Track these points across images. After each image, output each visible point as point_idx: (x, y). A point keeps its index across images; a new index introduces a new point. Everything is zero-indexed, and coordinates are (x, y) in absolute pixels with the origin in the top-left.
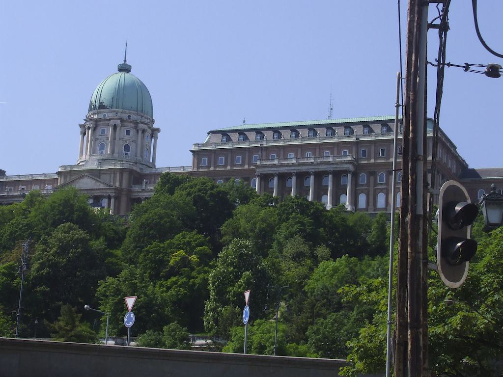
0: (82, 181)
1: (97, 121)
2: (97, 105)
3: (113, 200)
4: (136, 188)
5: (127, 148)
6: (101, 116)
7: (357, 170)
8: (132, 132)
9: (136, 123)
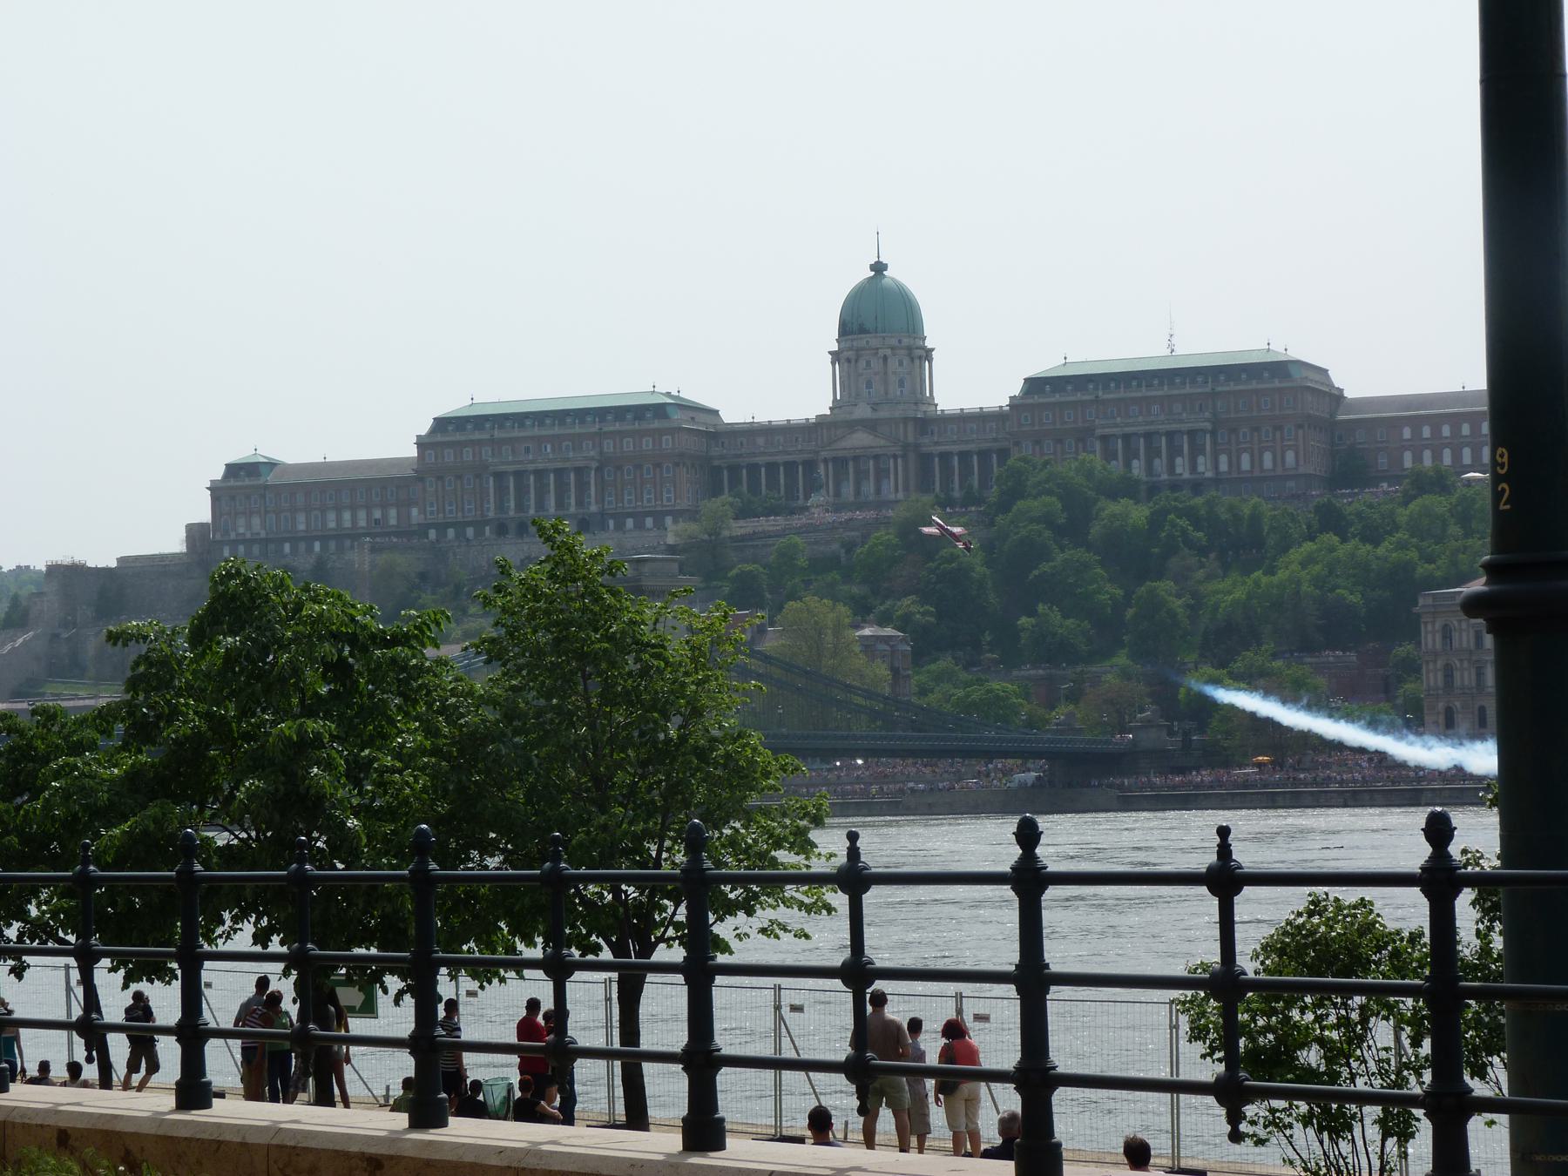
1: (858, 350)
4: (926, 440)
5: (901, 383)
9: (910, 349)
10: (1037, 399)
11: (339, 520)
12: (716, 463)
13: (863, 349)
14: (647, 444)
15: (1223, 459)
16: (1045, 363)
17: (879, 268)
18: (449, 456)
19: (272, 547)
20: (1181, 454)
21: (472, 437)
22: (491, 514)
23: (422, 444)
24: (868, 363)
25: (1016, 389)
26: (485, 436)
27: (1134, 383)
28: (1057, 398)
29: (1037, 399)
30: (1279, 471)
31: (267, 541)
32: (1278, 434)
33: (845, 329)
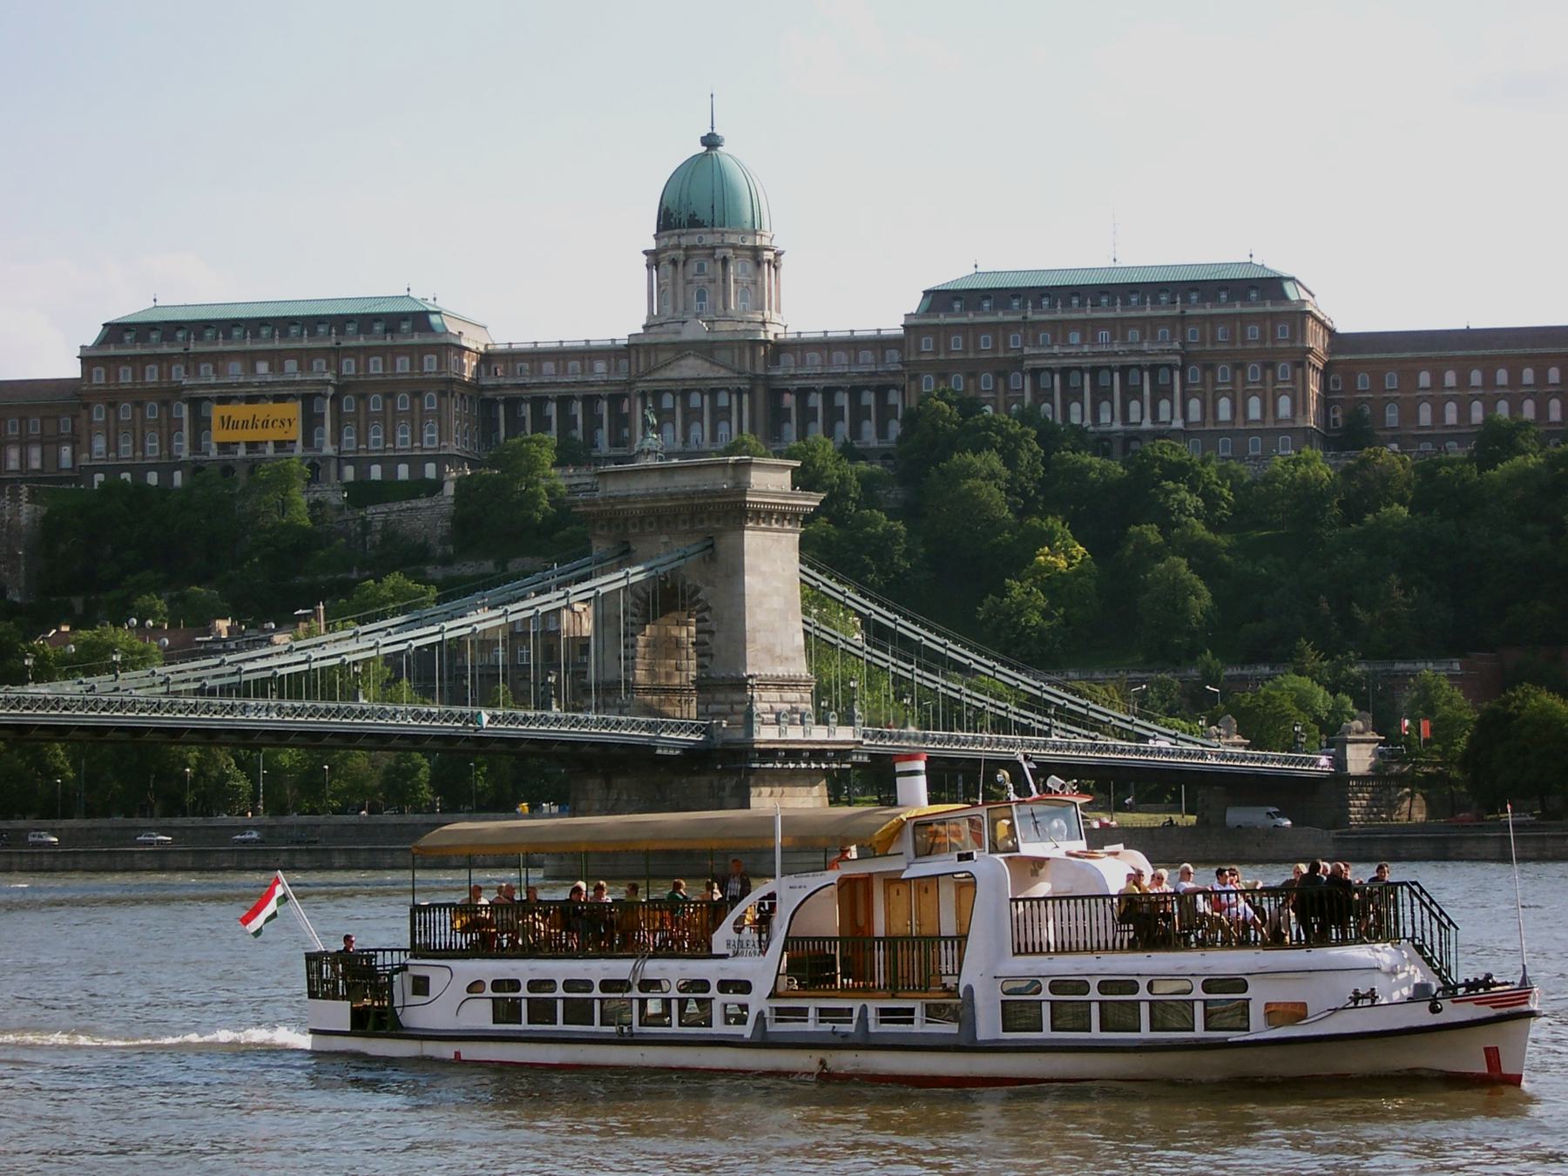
0: (683, 362)
1: (687, 248)
2: (684, 219)
3: (746, 398)
6: (694, 240)
7: (1187, 357)
8: (750, 266)
9: (756, 251)
10: (943, 319)
12: (489, 394)
13: (695, 247)
15: (1195, 405)
16: (950, 272)
17: (711, 142)
18: (126, 376)
20: (1139, 395)
21: (158, 351)
22: (185, 455)
23: (87, 359)
24: (701, 268)
25: (913, 303)
26: (180, 350)
27: (1075, 301)
28: (971, 317)
29: (943, 319)
30: (1270, 425)
32: (1269, 373)
33: (667, 221)
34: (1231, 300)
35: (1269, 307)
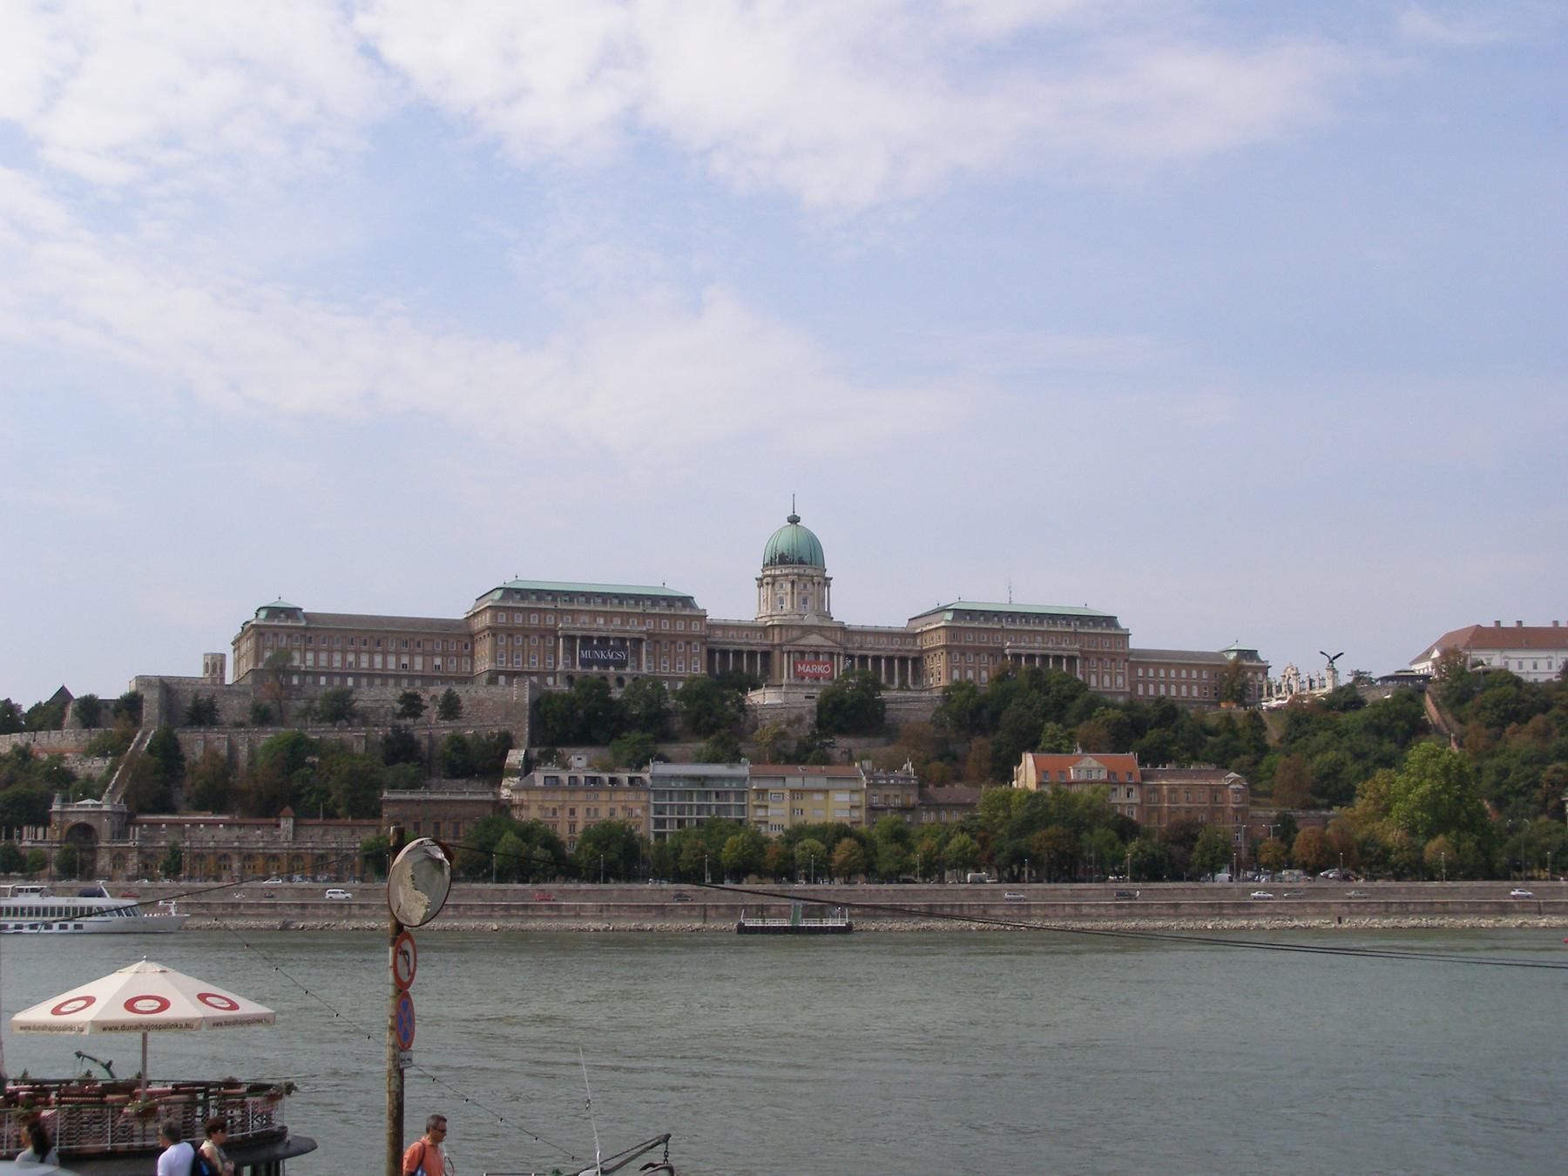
11: (371, 662)
14: (680, 627)
17: (794, 520)
18: (519, 620)
19: (309, 679)
31: (306, 673)
34: (1095, 625)
35: (1113, 631)
